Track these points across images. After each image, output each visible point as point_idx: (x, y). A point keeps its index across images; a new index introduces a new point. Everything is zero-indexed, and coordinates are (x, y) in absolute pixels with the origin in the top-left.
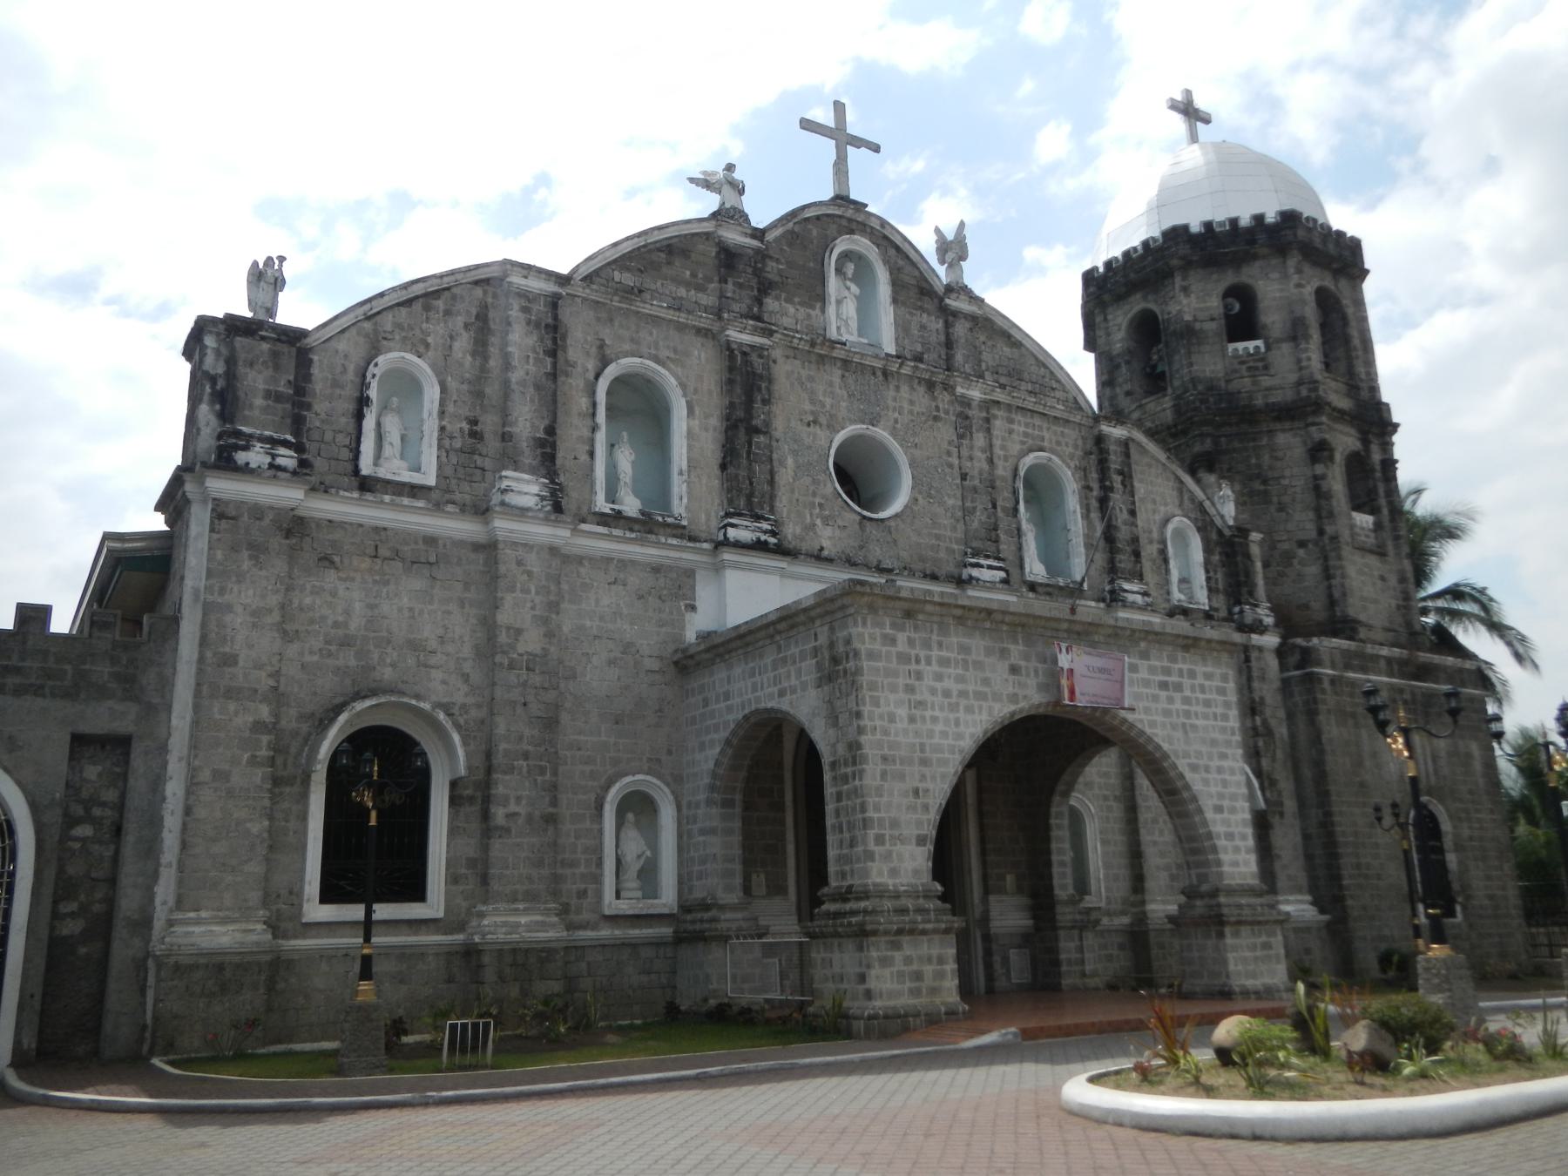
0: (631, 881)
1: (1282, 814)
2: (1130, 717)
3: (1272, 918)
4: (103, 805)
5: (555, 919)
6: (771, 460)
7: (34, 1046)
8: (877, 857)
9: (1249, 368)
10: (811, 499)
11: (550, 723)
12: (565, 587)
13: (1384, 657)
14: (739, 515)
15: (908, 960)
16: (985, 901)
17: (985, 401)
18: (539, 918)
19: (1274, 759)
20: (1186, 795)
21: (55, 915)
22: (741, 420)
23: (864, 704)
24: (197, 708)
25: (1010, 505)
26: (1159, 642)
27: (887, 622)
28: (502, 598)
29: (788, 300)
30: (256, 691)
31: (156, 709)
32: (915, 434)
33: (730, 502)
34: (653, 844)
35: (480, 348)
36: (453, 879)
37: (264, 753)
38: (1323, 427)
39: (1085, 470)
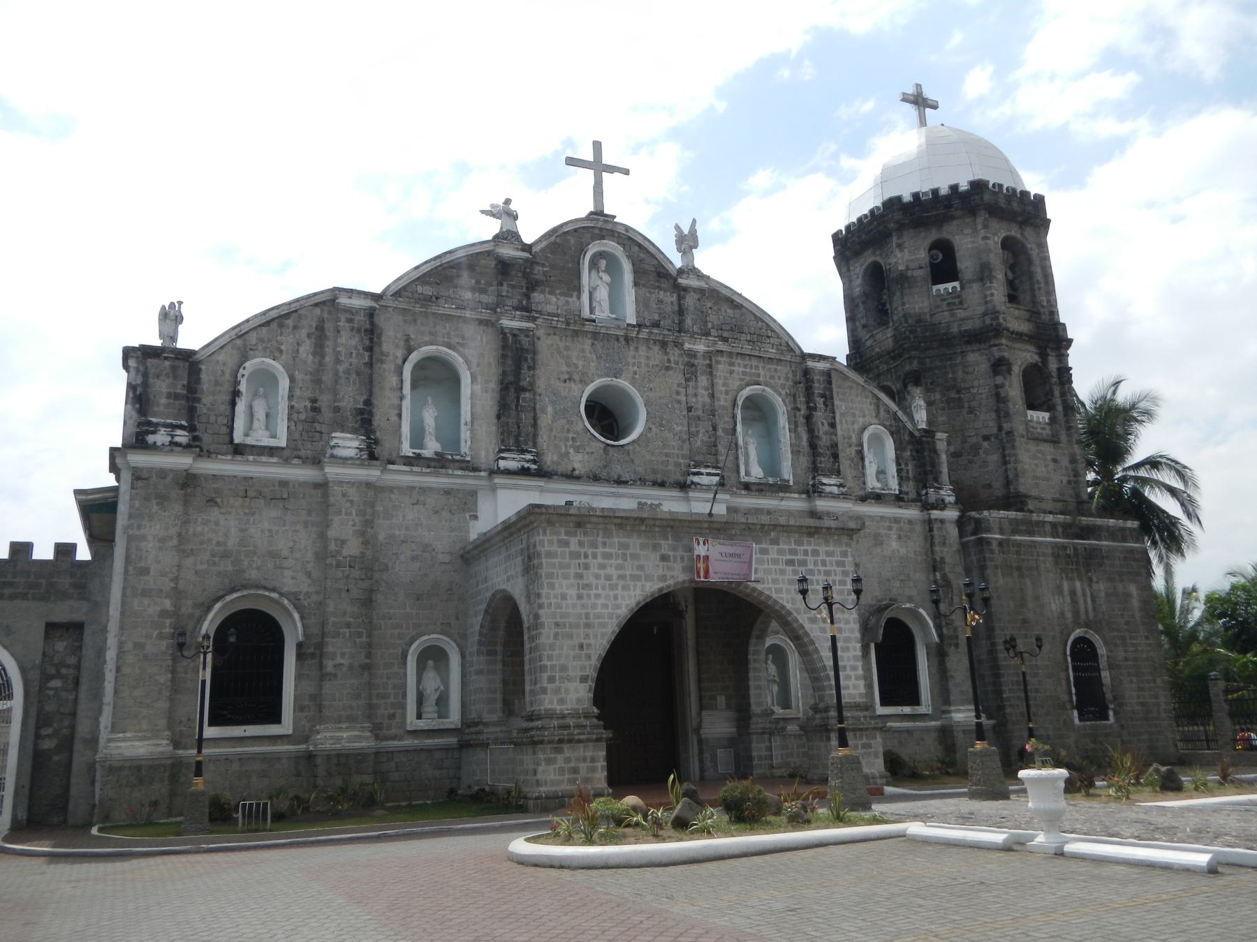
0: (430, 708)
1: (957, 646)
2: (759, 587)
3: (870, 726)
4: (68, 666)
5: (369, 734)
6: (534, 409)
7: (25, 817)
8: (549, 691)
9: (949, 304)
10: (567, 435)
11: (368, 602)
12: (379, 508)
13: (1050, 522)
14: (509, 450)
15: (568, 760)
16: (699, 714)
17: (708, 352)
18: (357, 733)
19: (951, 604)
20: (806, 640)
21: (38, 736)
22: (511, 383)
23: (542, 588)
24: (123, 604)
25: (730, 427)
27: (563, 530)
28: (331, 520)
29: (549, 293)
30: (161, 590)
31: (100, 606)
32: (650, 381)
33: (503, 441)
34: (446, 682)
35: (319, 350)
36: (299, 708)
37: (168, 630)
38: (1004, 347)
39: (794, 396)
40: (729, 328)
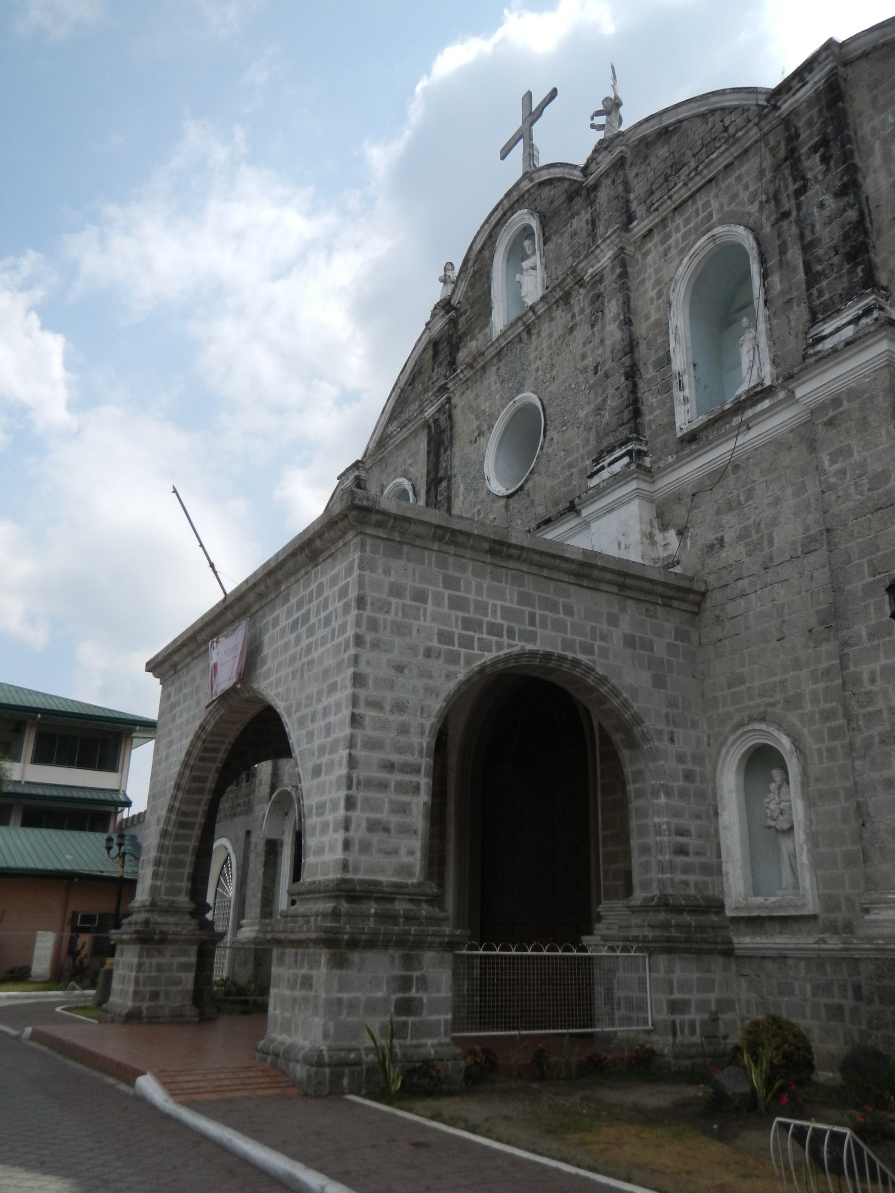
26: (288, 576)
40: (661, 180)
